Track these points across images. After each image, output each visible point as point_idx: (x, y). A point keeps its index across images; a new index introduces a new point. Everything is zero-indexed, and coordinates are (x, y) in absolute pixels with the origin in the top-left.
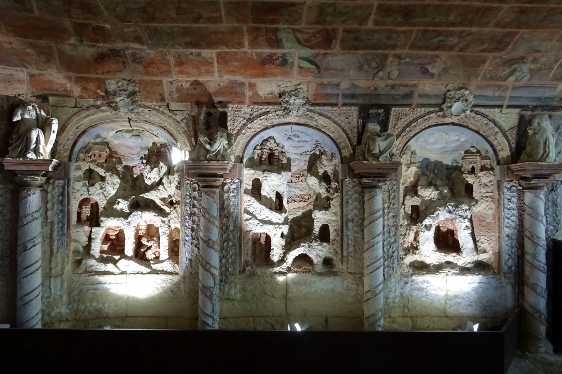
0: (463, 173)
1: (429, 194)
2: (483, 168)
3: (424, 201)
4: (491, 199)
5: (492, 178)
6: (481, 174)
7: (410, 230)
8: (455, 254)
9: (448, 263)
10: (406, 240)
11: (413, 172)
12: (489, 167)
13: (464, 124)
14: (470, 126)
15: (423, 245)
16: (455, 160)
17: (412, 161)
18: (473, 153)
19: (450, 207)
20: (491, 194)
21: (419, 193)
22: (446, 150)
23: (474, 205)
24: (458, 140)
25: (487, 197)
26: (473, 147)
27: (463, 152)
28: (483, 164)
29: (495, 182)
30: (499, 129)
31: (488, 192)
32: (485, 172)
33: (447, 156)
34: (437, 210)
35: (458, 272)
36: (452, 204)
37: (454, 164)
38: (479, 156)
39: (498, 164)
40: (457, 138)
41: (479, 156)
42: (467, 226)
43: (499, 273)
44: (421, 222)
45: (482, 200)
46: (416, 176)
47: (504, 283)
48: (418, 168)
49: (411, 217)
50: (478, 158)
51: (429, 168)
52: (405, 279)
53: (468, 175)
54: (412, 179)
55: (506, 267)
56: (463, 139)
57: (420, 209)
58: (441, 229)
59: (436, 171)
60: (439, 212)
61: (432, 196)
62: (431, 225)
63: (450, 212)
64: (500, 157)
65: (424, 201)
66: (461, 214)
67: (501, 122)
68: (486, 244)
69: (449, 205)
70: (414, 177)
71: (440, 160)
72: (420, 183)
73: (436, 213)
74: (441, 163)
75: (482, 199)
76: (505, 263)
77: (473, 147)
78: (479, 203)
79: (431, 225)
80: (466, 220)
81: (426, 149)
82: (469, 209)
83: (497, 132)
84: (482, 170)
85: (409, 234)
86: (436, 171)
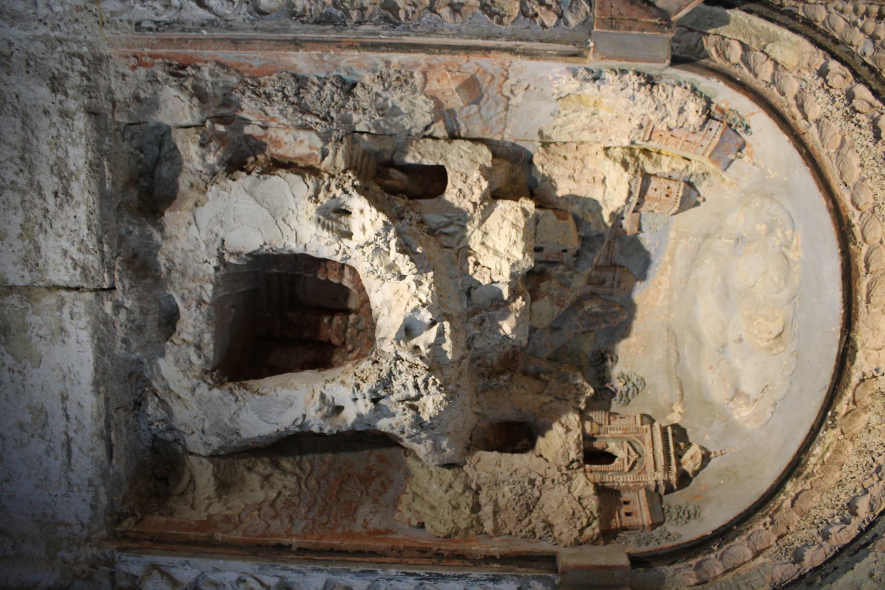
0: (584, 416)
1: (499, 246)
2: (608, 495)
3: (460, 219)
4: (463, 525)
5: (565, 531)
6: (582, 484)
7: (325, 138)
8: (209, 350)
9: (170, 320)
10: (273, 111)
11: (597, 194)
12: (615, 523)
13: (842, 407)
14: (829, 436)
15: (250, 193)
16: (637, 387)
17: (654, 183)
18: (679, 457)
19: (430, 336)
20: (488, 526)
21: (503, 205)
22: (686, 351)
23: (437, 448)
24: (737, 393)
25: (476, 507)
26: (706, 458)
27: (676, 418)
28: (626, 496)
29: (546, 546)
30: (816, 569)
31: (495, 513)
32: (592, 503)
33: (659, 355)
34: (422, 269)
35: (119, 348)
36: (447, 346)
37: (619, 385)
38: (667, 483)
39: (636, 561)
40: (749, 387)
41: (667, 483)
42: (339, 409)
43: (114, 537)
44: (363, 191)
45: (458, 487)
46: (576, 209)
47: (69, 556)
48: (617, 217)
49: (391, 164)
50: (655, 476)
51: (608, 275)
52: (75, 79)
53: (576, 433)
54: (563, 188)
55: (136, 569)
56: (742, 413)
57: (426, 203)
58: (337, 320)
59: (591, 306)
60: (410, 279)
61: (488, 260)
62: (349, 235)
63: (408, 331)
64: (668, 570)
65: (460, 219)
66: (396, 385)
67: (849, 576)
68: (259, 495)
69: (441, 334)
70: (573, 199)
71: (638, 325)
72: (549, 217)
73: (405, 264)
74: (623, 330)
75: (467, 487)
76: (155, 567)
77: (706, 458)
78: (448, 474)
79: (349, 235)
80: (364, 407)
81: (694, 261)
82: (419, 424)
83: (798, 558)
84: (601, 490)
85: (305, 127)
86: (591, 306)
